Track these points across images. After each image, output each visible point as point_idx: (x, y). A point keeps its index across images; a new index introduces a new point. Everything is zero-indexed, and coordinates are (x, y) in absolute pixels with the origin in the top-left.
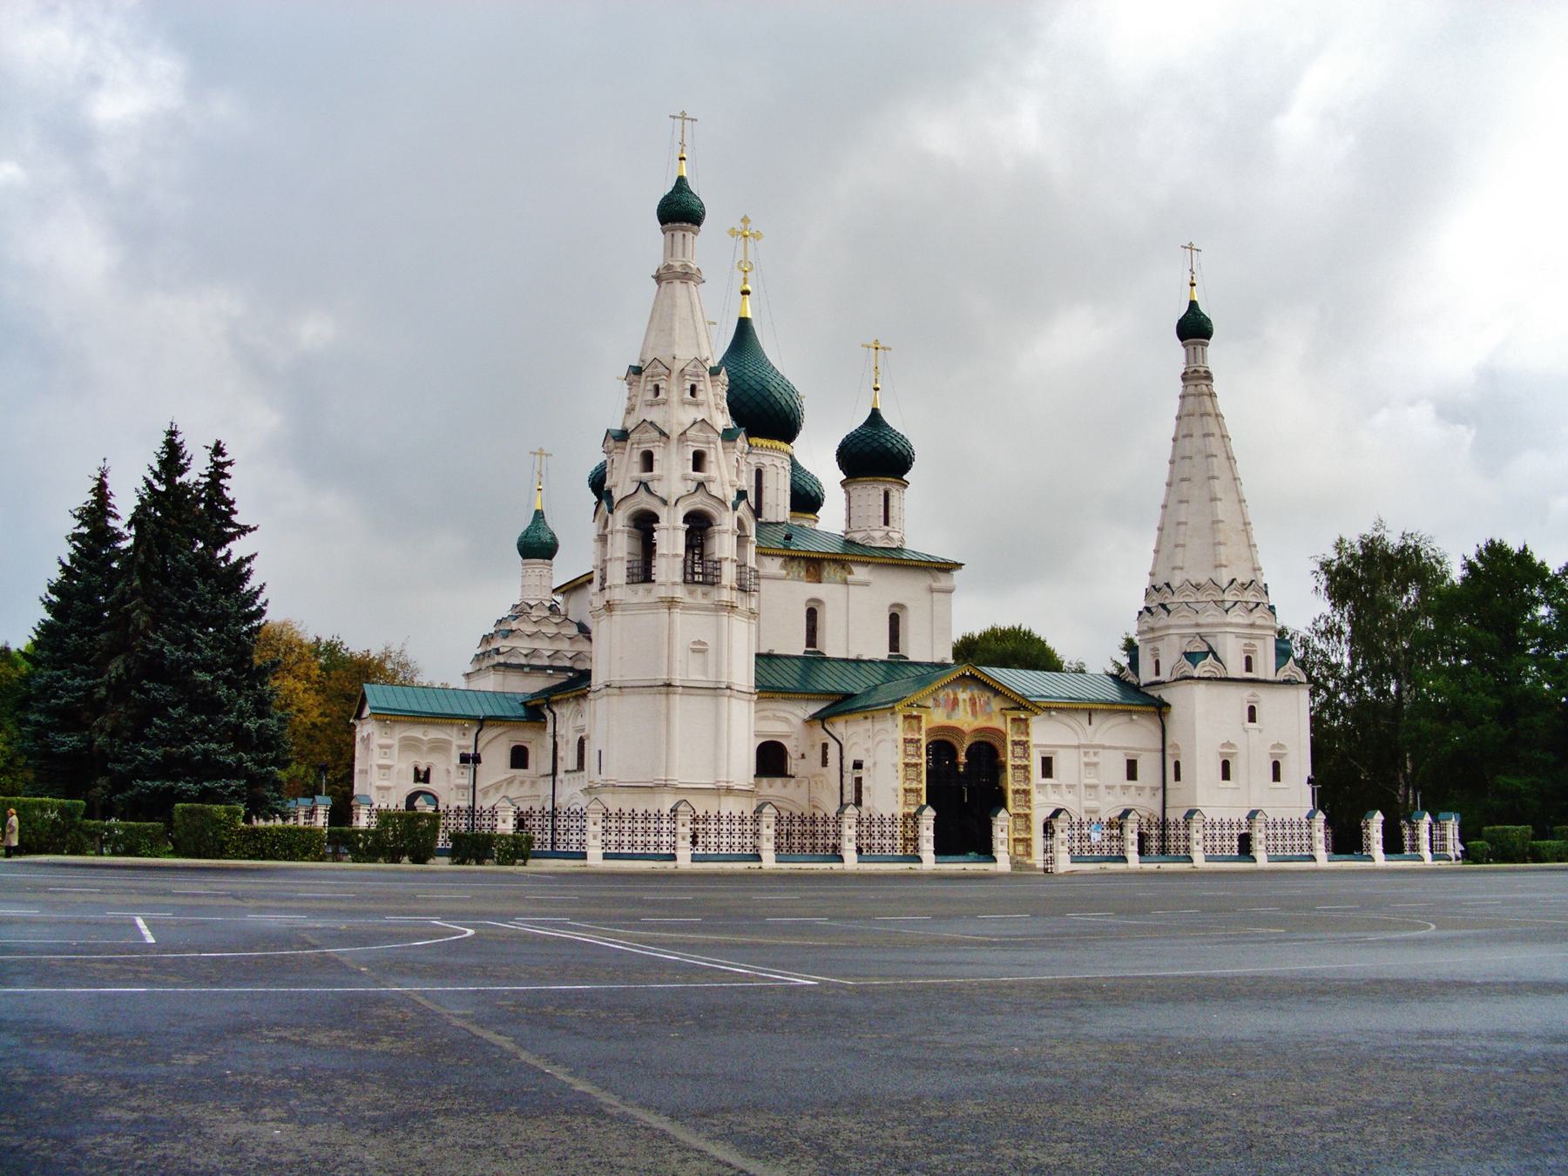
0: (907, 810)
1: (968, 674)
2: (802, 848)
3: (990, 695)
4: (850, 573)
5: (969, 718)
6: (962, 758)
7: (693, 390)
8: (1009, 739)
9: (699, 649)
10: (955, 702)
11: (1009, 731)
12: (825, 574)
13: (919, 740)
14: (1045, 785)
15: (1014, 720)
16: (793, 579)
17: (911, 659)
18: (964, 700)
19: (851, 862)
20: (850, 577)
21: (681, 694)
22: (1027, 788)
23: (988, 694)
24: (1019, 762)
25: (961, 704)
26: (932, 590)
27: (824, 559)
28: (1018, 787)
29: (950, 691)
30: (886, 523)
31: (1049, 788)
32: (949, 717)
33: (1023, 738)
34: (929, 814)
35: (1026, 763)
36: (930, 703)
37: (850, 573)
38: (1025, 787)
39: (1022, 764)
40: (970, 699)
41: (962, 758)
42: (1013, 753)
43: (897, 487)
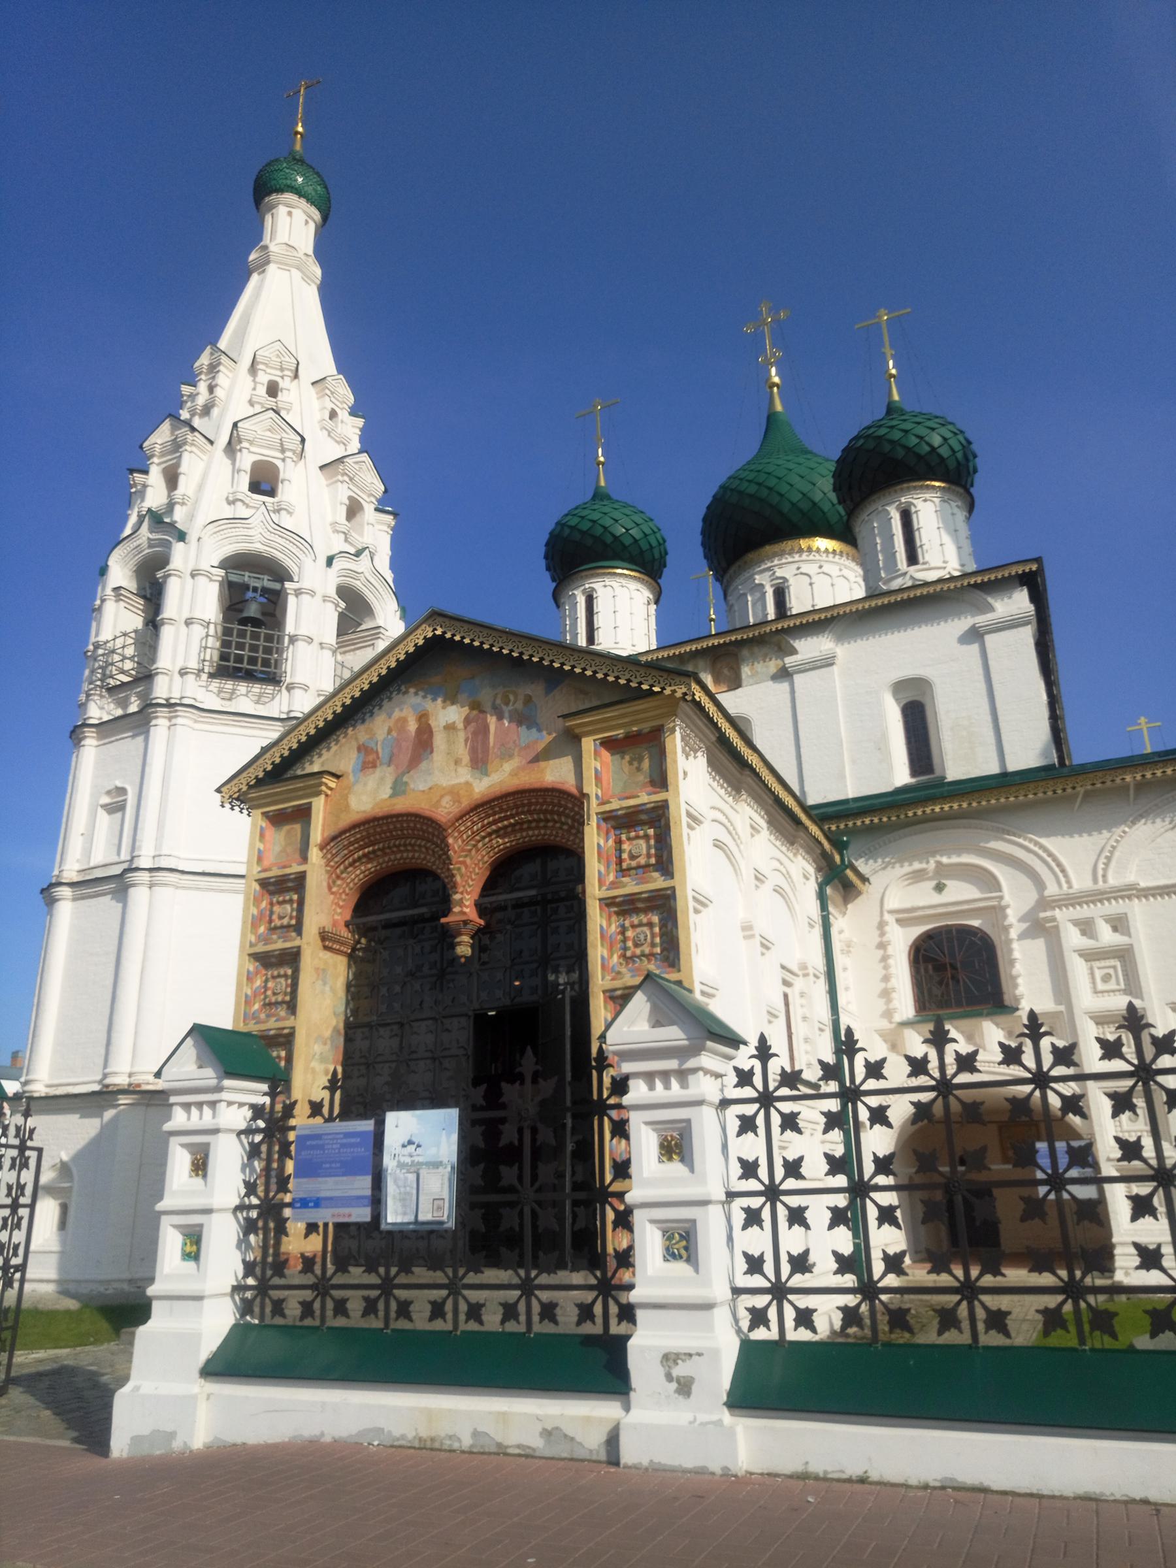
3: (535, 690)
4: (794, 652)
5: (465, 775)
10: (424, 741)
11: (590, 788)
12: (746, 671)
18: (450, 728)
20: (789, 660)
21: (75, 899)
24: (630, 886)
25: (439, 740)
32: (399, 788)
37: (794, 652)
43: (927, 496)
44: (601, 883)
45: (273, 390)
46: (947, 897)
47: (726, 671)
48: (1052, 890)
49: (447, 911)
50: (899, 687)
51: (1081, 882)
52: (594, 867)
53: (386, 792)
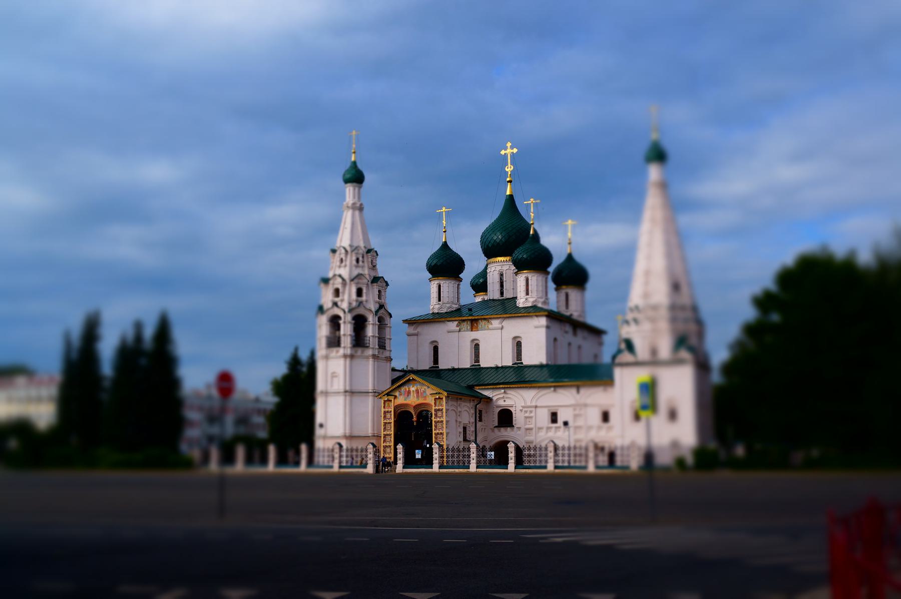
0: (384, 444)
1: (411, 378)
2: (485, 462)
3: (426, 388)
4: (491, 324)
5: (416, 399)
6: (415, 419)
7: (342, 260)
8: (434, 408)
9: (334, 375)
10: (409, 392)
13: (391, 411)
14: (551, 428)
15: (435, 399)
16: (464, 331)
17: (524, 363)
18: (413, 391)
19: (473, 468)
20: (490, 326)
22: (442, 432)
23: (425, 387)
24: (438, 419)
26: (536, 327)
27: (479, 319)
28: (437, 431)
29: (407, 387)
30: (527, 294)
31: (553, 430)
33: (440, 408)
34: (400, 447)
35: (442, 420)
36: (397, 394)
37: (491, 324)
38: (441, 431)
39: (440, 420)
40: (416, 390)
41: (415, 419)
42: (436, 415)
44: (435, 418)
45: (358, 261)
46: (506, 403)
47: (475, 325)
48: (523, 404)
49: (413, 418)
50: (515, 338)
51: (529, 404)
52: (433, 416)
53: (404, 399)
